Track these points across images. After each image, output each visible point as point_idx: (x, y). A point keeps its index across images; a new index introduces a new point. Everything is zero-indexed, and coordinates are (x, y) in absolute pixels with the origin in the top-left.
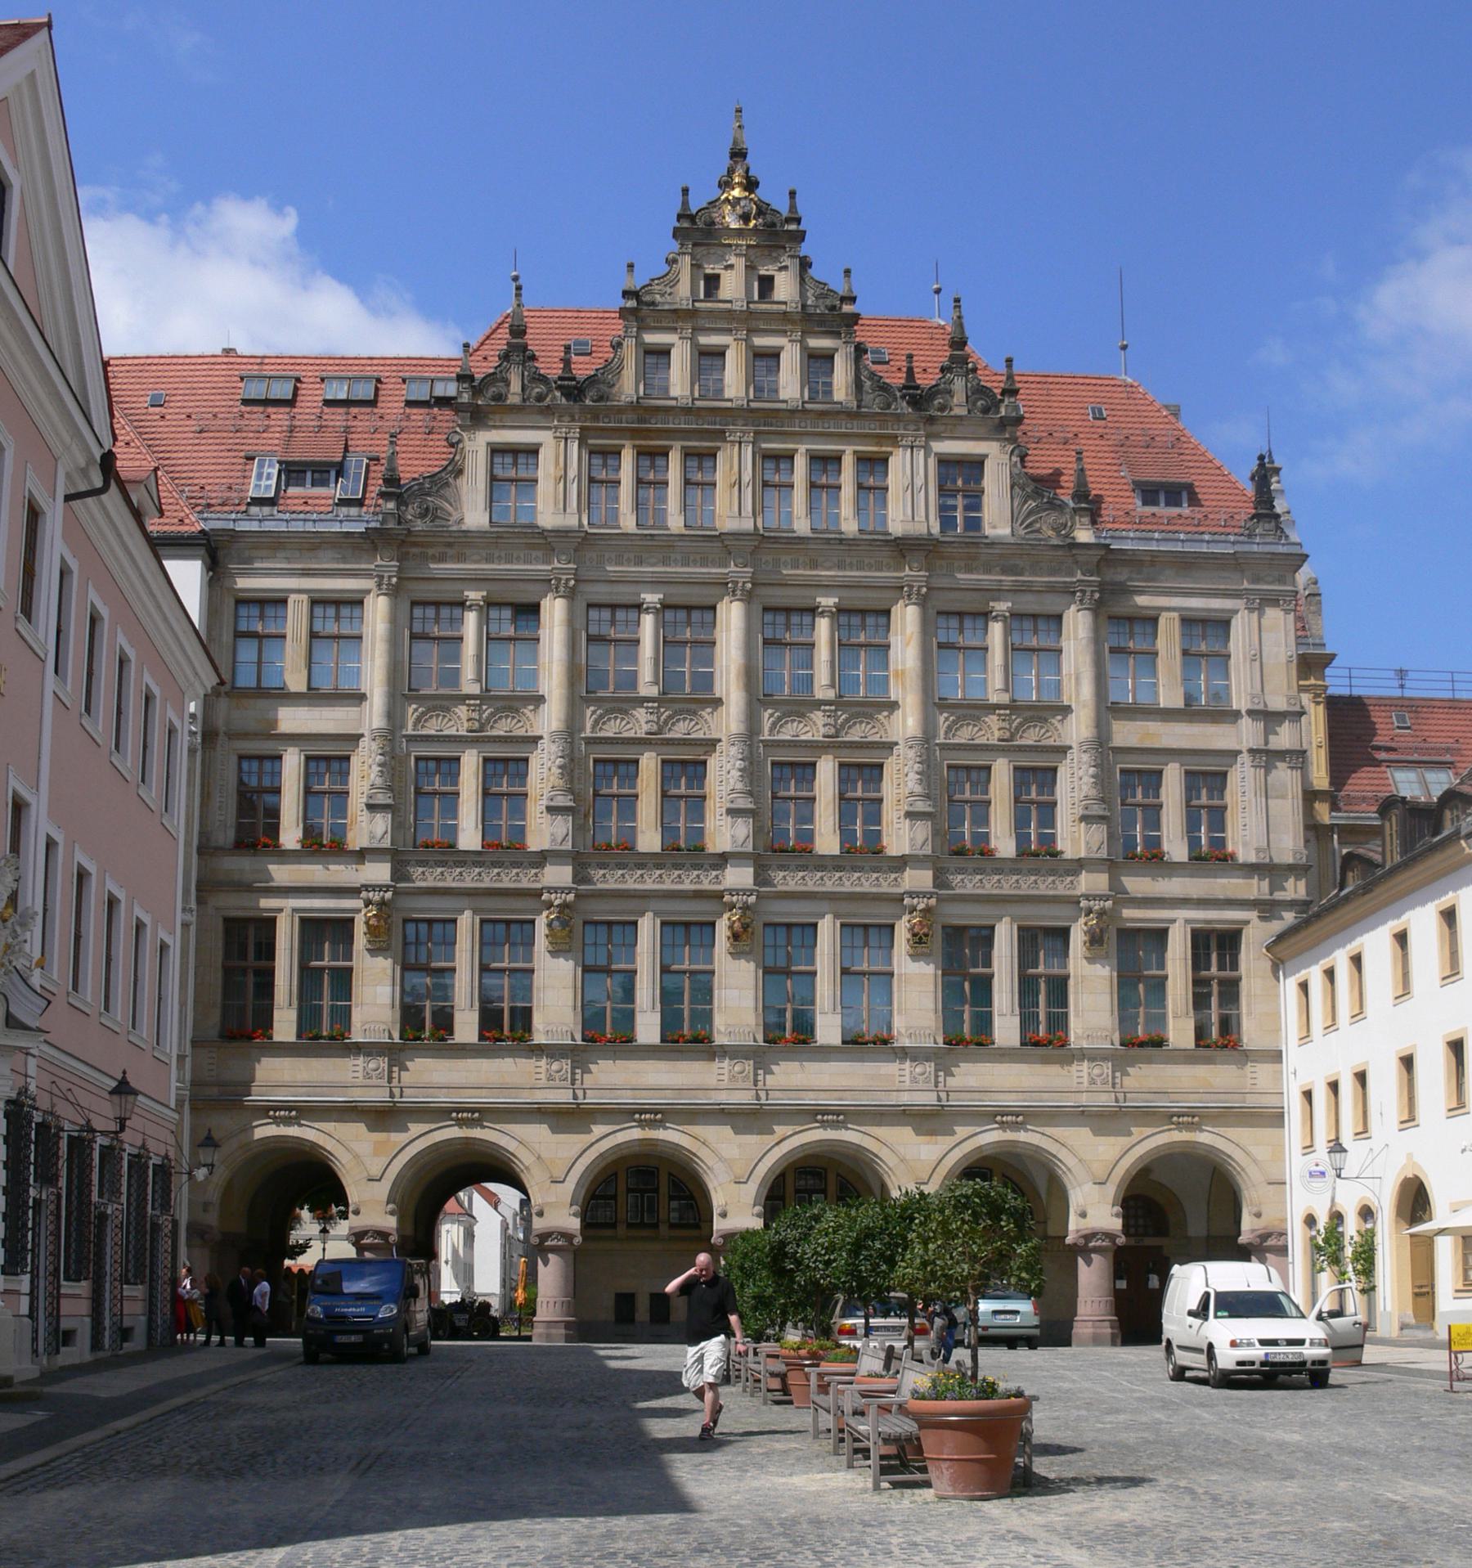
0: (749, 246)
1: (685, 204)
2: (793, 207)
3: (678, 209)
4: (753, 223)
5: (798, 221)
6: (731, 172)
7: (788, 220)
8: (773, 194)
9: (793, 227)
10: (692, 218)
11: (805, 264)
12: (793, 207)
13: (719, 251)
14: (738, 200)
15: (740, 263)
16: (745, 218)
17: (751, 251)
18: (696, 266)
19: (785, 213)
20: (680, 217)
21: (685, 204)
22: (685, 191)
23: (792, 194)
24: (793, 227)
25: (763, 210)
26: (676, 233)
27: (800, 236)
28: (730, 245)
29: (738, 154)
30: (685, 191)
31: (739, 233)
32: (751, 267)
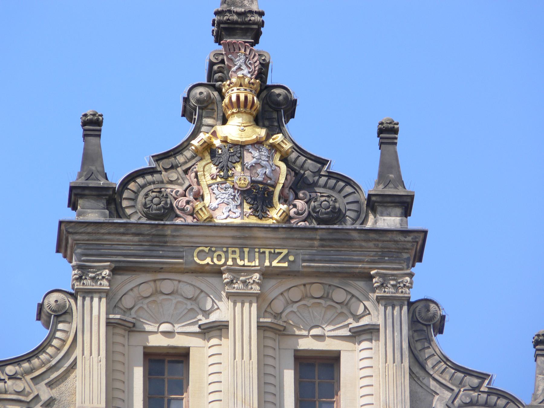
0: (267, 274)
1: (91, 159)
2: (389, 169)
3: (71, 172)
4: (277, 212)
5: (405, 204)
6: (217, 74)
7: (375, 204)
8: (334, 133)
9: (389, 221)
10: (111, 198)
11: (425, 322)
12: (389, 169)
13: (188, 286)
14: (239, 148)
15: (243, 319)
16: (258, 196)
17: (275, 288)
18: (122, 327)
19: (368, 183)
20: (76, 194)
21: (91, 159)
22: (92, 125)
23: (388, 133)
24: (389, 221)
25: (306, 175)
26: (67, 239)
27: (411, 247)
28: (217, 272)
29: (237, 28)
30: (92, 125)
31: (241, 237)
32: (272, 331)
